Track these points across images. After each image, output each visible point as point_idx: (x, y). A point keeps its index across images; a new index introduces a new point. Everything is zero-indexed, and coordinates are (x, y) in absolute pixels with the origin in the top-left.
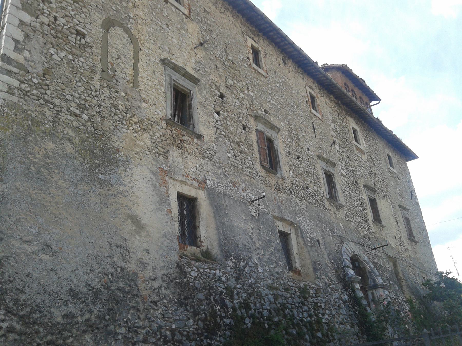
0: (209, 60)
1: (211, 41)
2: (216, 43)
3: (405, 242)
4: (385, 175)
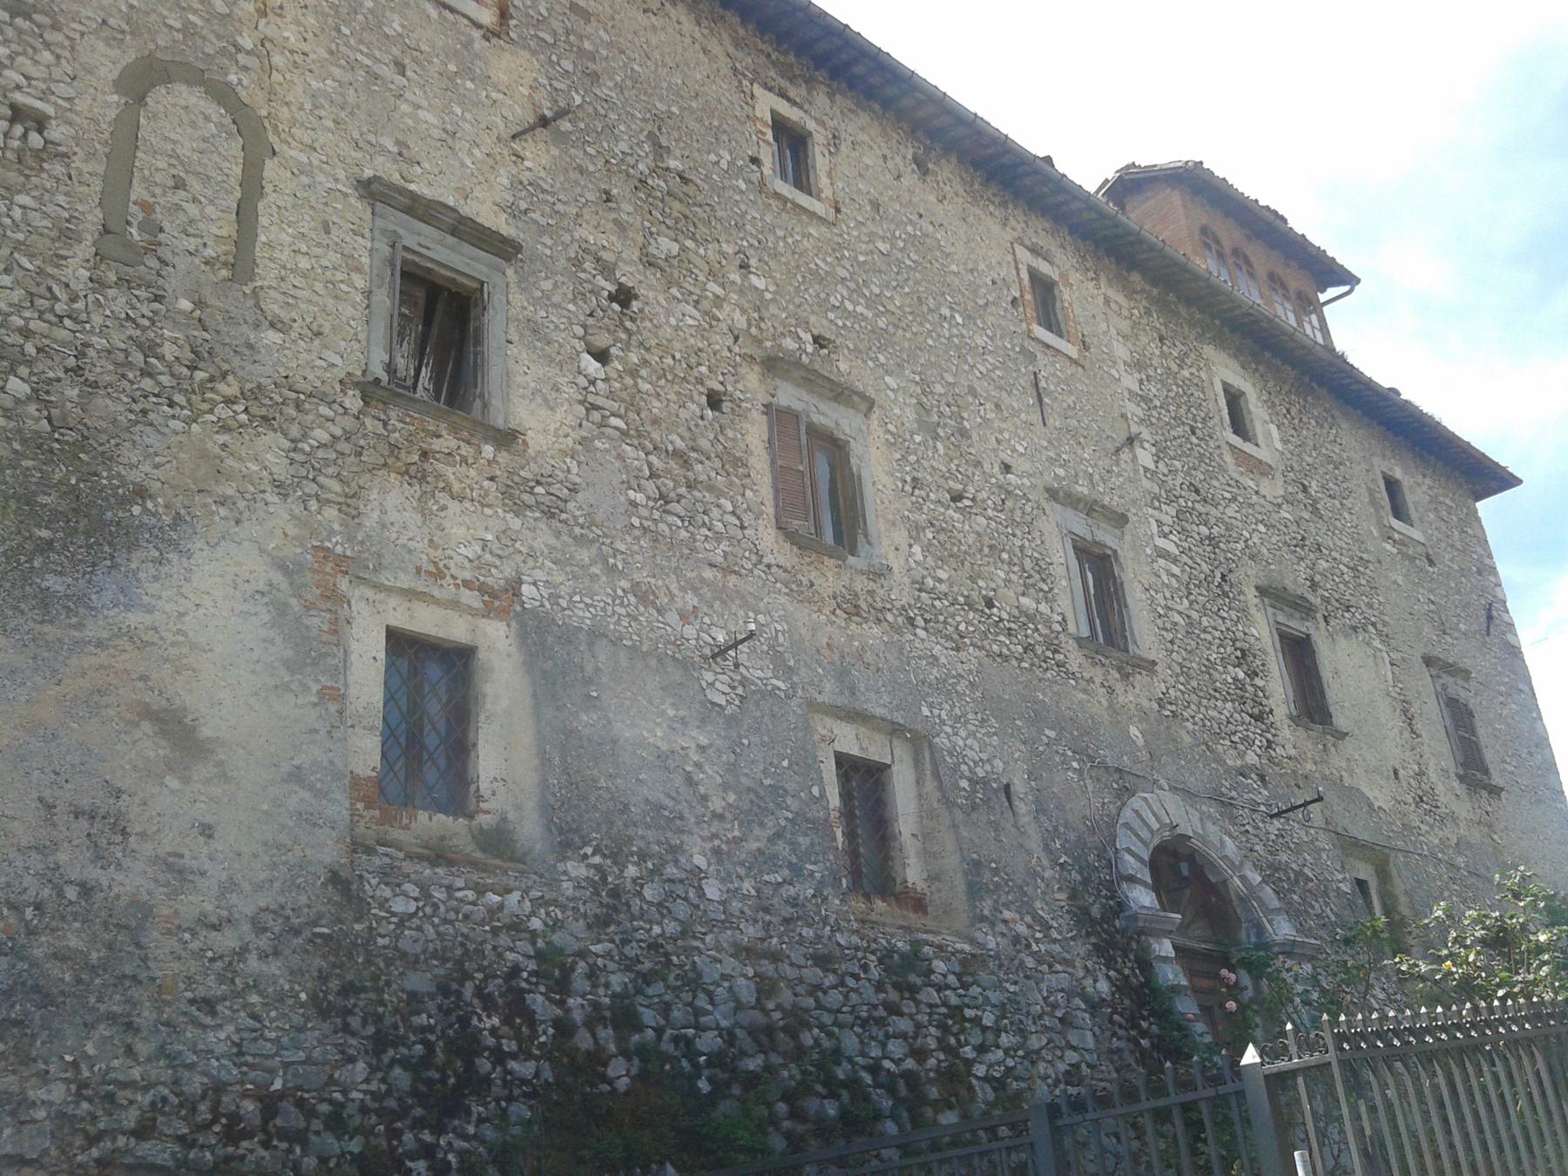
0: (574, 175)
1: (591, 110)
2: (613, 116)
3: (1440, 789)
4: (1366, 551)
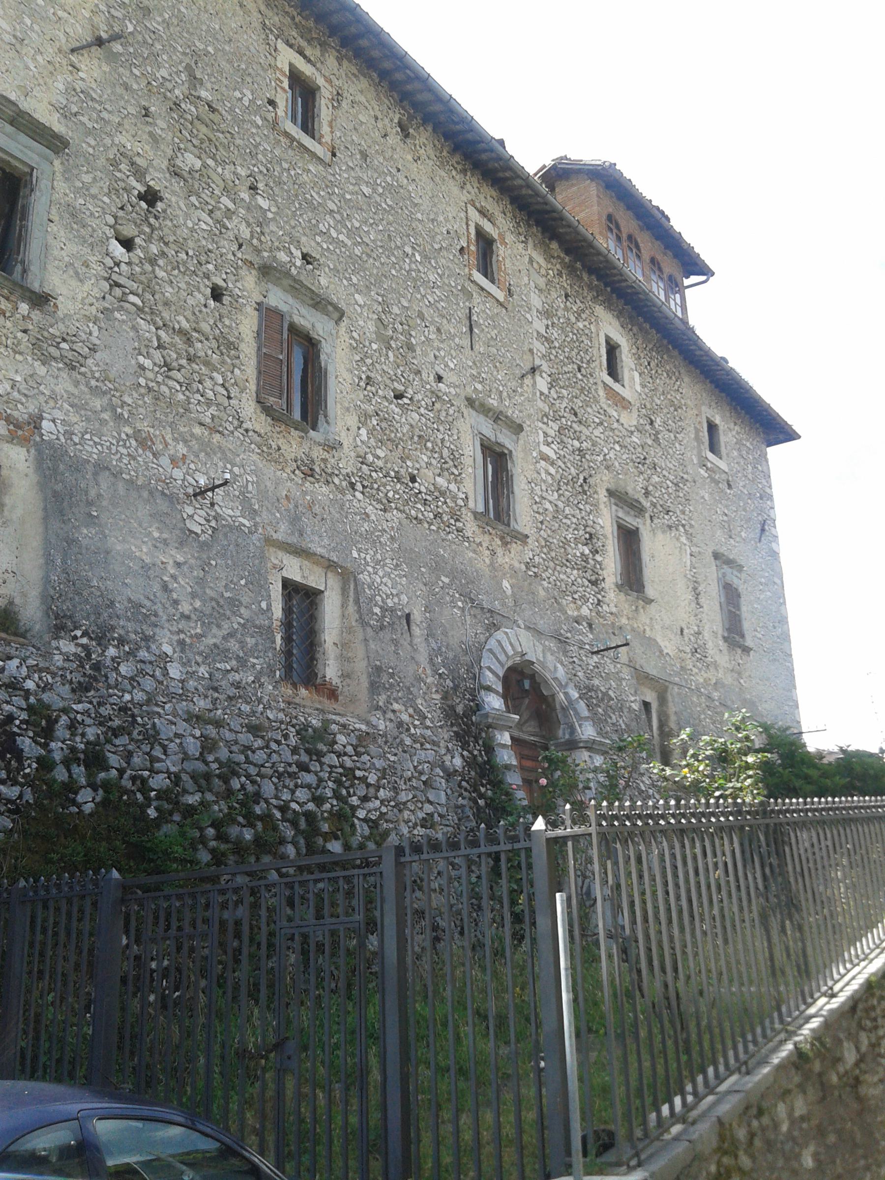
0: (120, 90)
1: (140, 38)
2: (159, 46)
3: (710, 645)
4: (687, 473)
